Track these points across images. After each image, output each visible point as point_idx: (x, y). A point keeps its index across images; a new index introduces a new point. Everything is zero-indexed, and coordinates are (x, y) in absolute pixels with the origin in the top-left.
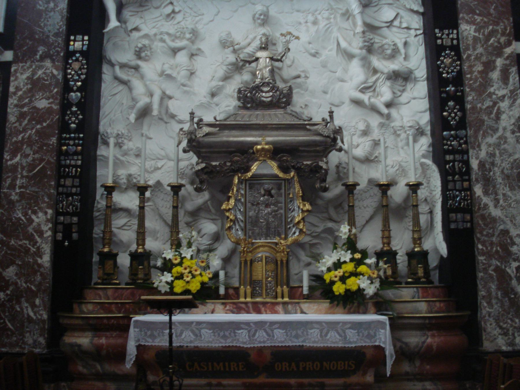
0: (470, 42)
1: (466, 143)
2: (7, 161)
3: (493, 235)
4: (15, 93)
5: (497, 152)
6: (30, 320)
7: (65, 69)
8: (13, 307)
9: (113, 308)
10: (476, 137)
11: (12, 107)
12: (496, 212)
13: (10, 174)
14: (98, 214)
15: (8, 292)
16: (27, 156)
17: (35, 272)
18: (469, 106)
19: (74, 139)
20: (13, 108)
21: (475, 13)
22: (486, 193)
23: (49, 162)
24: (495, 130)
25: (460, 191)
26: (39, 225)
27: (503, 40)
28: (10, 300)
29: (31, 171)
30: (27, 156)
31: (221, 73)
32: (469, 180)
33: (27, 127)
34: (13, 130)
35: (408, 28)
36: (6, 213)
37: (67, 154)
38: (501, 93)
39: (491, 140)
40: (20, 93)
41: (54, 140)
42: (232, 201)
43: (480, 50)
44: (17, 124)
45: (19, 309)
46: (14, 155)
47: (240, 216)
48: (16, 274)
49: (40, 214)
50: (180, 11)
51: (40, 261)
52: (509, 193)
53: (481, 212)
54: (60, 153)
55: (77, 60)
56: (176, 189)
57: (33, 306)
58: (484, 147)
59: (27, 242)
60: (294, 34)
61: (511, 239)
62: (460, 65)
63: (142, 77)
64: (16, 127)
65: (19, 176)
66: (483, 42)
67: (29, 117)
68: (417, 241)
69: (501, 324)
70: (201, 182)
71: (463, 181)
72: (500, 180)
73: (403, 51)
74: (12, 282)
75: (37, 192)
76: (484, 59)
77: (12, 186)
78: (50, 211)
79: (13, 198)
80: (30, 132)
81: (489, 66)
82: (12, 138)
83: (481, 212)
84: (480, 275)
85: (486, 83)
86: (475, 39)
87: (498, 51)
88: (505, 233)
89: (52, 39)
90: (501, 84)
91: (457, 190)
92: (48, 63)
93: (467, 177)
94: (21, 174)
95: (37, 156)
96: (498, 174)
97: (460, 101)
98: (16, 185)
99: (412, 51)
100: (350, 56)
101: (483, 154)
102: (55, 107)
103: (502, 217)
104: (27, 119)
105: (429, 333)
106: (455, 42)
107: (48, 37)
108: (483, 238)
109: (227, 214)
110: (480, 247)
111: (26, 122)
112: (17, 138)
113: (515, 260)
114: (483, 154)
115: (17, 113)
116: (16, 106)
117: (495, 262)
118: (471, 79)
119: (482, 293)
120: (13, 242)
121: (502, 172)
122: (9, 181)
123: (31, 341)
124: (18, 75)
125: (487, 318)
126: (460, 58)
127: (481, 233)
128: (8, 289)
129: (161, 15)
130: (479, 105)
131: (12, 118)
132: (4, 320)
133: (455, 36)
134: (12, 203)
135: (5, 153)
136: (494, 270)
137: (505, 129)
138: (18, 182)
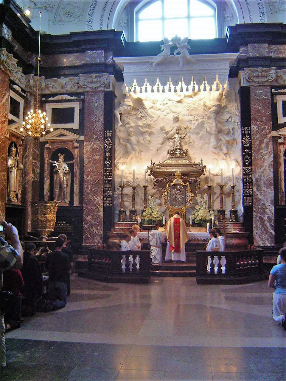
0: (255, 132)
1: (251, 171)
3: (259, 205)
4: (86, 153)
5: (262, 175)
6: (97, 234)
7: (104, 144)
8: (90, 230)
9: (126, 230)
10: (255, 170)
12: (260, 197)
14: (116, 196)
15: (88, 225)
16: (92, 177)
17: (98, 218)
18: (253, 158)
19: (109, 170)
21: (258, 121)
22: (257, 190)
23: (100, 179)
24: (262, 167)
25: (248, 189)
26: (98, 201)
27: (267, 131)
29: (94, 182)
30: (92, 177)
31: (160, 142)
32: (252, 185)
35: (235, 122)
37: (106, 175)
38: (265, 153)
39: (260, 170)
40: (88, 153)
41: (102, 171)
42: (166, 193)
43: (258, 136)
46: (87, 177)
47: (169, 198)
48: (91, 219)
49: (98, 198)
50: (144, 116)
51: (99, 214)
52: (266, 190)
53: (255, 197)
54: (104, 175)
55: (108, 140)
56: (145, 188)
57: (97, 229)
58: (257, 173)
59: (94, 207)
60: (189, 127)
61: (266, 207)
62: (251, 141)
63: (130, 143)
66: (260, 133)
68: (234, 206)
69: (261, 237)
70: (155, 186)
71: (249, 185)
72: (263, 185)
73: (232, 132)
75: (96, 190)
76: (260, 139)
77: (88, 188)
78: (102, 197)
81: (261, 142)
83: (255, 197)
84: (254, 219)
85: (260, 149)
86: (257, 132)
87: (265, 136)
88: (264, 204)
89: (99, 132)
90: (265, 148)
91: (247, 189)
92: (98, 142)
93: (251, 184)
95: (96, 176)
96: (262, 183)
97: (250, 155)
99: (236, 130)
100: (211, 134)
101: (257, 176)
102: (102, 159)
103: (263, 199)
105: (234, 239)
106: (249, 132)
107: (97, 132)
108: (255, 206)
109: (165, 197)
110: (254, 209)
113: (267, 214)
114: (257, 176)
117: (259, 215)
118: (254, 147)
119: (254, 226)
120: (89, 207)
121: (264, 182)
122: (86, 186)
123: (97, 241)
125: (256, 234)
126: (251, 139)
127: (255, 204)
128: (88, 223)
129: (137, 118)
130: (257, 157)
131: (86, 163)
133: (249, 130)
134: (88, 194)
136: (259, 218)
137: (266, 166)
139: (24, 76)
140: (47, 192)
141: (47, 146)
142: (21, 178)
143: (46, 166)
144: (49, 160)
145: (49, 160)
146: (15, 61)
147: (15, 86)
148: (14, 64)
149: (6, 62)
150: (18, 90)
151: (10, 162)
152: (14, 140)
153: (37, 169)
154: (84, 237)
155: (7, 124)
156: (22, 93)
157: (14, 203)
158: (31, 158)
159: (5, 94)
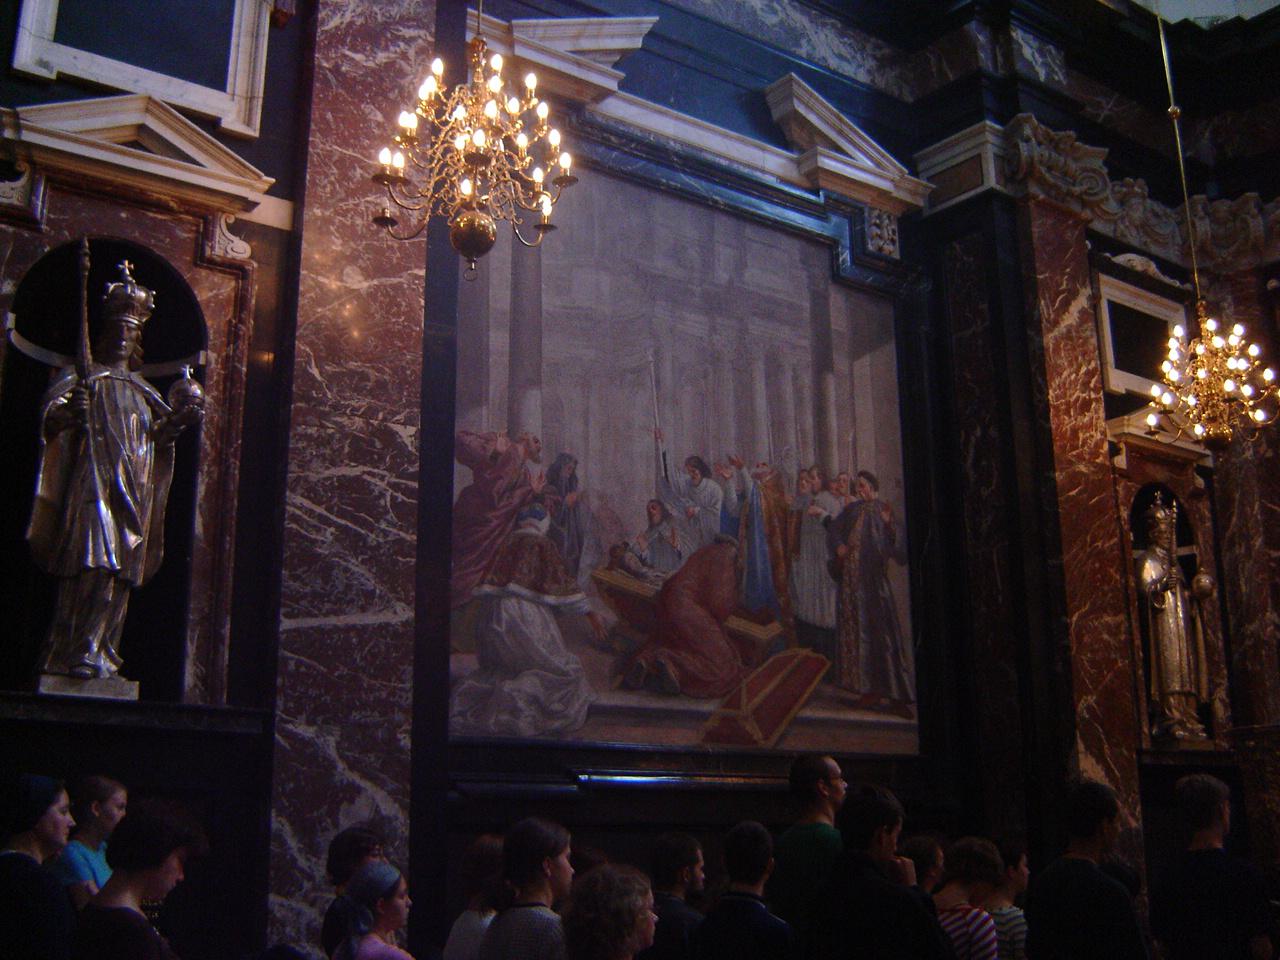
139: (1168, 211)
142: (1220, 635)
146: (1095, 158)
147: (1121, 259)
148: (1094, 171)
149: (1041, 162)
150: (1139, 268)
151: (1151, 571)
152: (1160, 474)
155: (1102, 414)
156: (1167, 280)
157: (1185, 746)
158: (1258, 542)
159: (1073, 294)
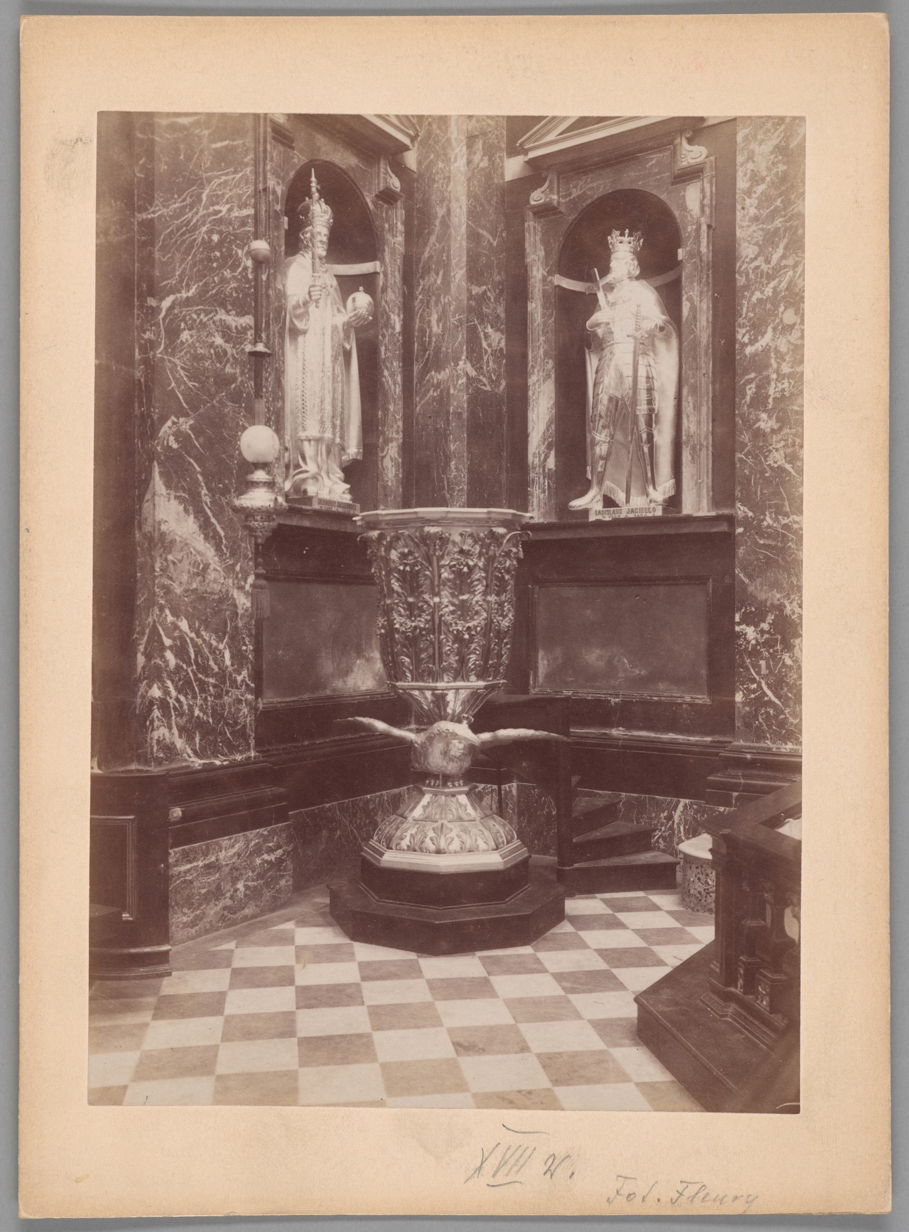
2: (744, 345)
4: (749, 193)
11: (746, 224)
13: (753, 375)
20: (749, 226)
28: (768, 644)
33: (784, 263)
34: (752, 276)
36: (750, 461)
40: (761, 188)
44: (760, 262)
45: (789, 662)
64: (757, 268)
65: (774, 376)
67: (785, 240)
74: (772, 604)
79: (762, 425)
80: (791, 273)
82: (753, 294)
94: (777, 371)
98: (768, 397)
104: (782, 246)
111: (780, 251)
112: (762, 292)
115: (759, 236)
116: (756, 219)
120: (768, 521)
122: (750, 390)
124: (754, 146)
132: (759, 685)
135: (738, 329)
138: (771, 391)
140: (543, 448)
141: (537, 197)
142: (399, 379)
143: (536, 308)
144: (550, 273)
145: (550, 273)
153: (489, 330)
154: (739, 697)
